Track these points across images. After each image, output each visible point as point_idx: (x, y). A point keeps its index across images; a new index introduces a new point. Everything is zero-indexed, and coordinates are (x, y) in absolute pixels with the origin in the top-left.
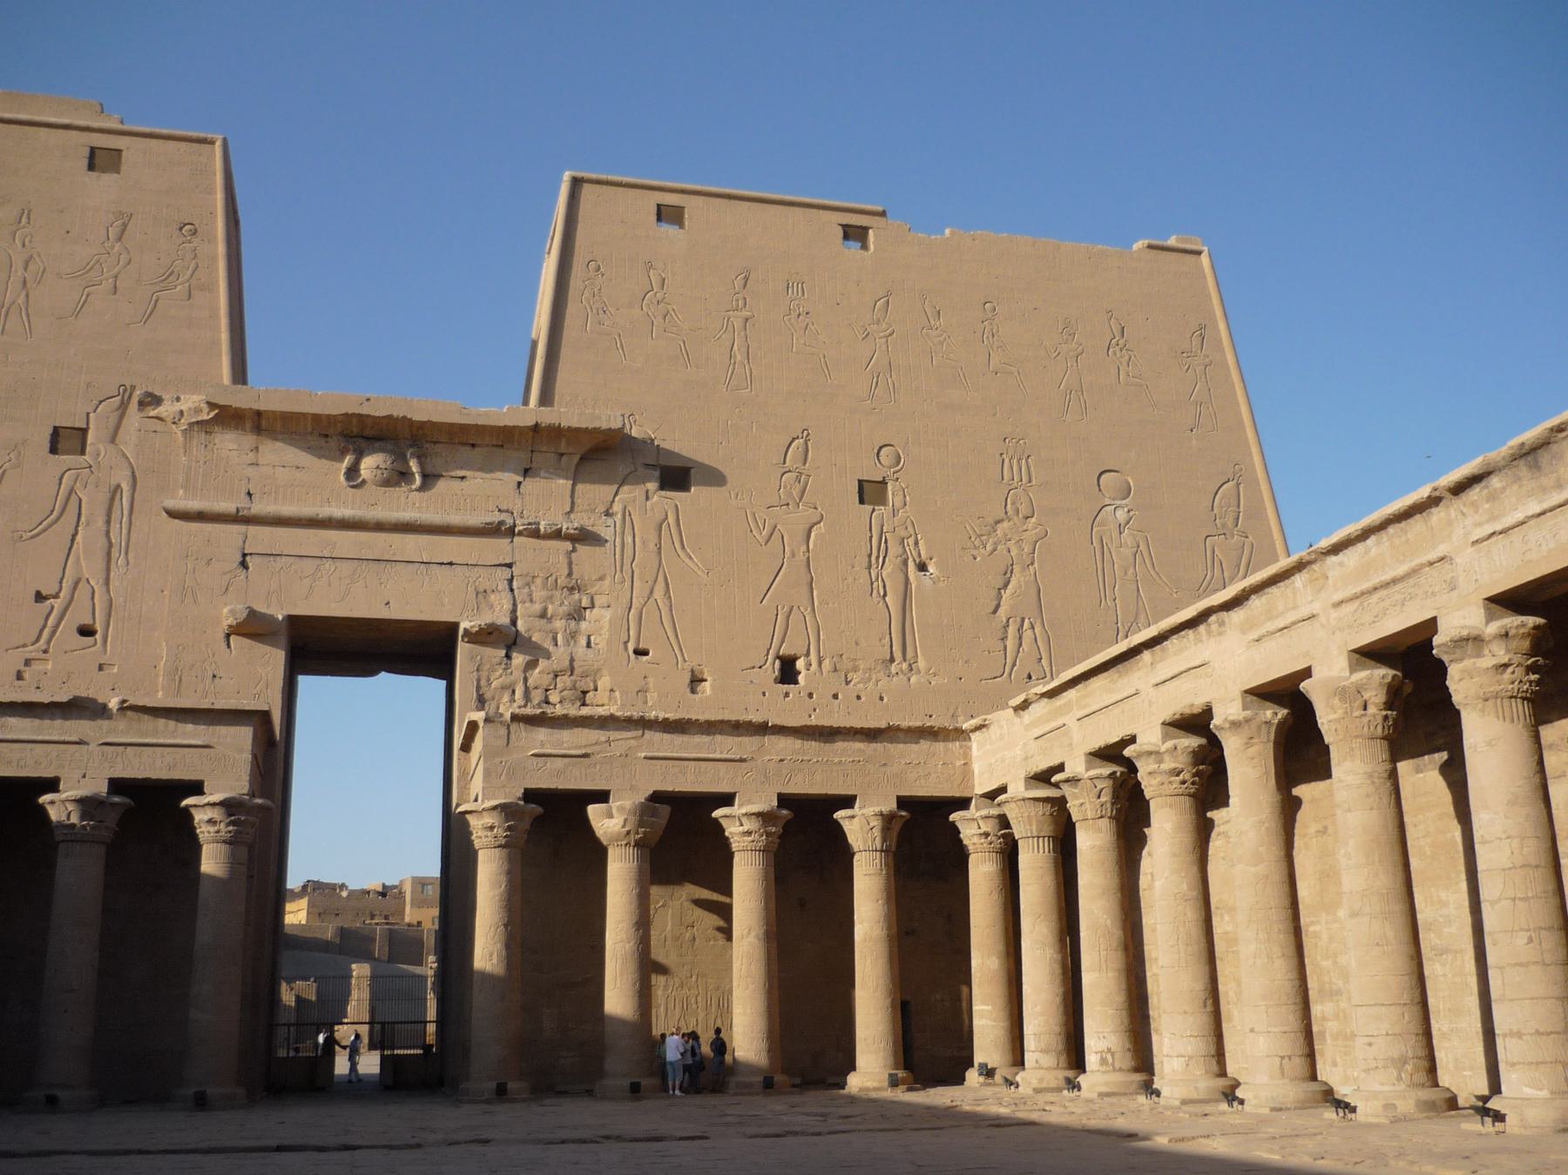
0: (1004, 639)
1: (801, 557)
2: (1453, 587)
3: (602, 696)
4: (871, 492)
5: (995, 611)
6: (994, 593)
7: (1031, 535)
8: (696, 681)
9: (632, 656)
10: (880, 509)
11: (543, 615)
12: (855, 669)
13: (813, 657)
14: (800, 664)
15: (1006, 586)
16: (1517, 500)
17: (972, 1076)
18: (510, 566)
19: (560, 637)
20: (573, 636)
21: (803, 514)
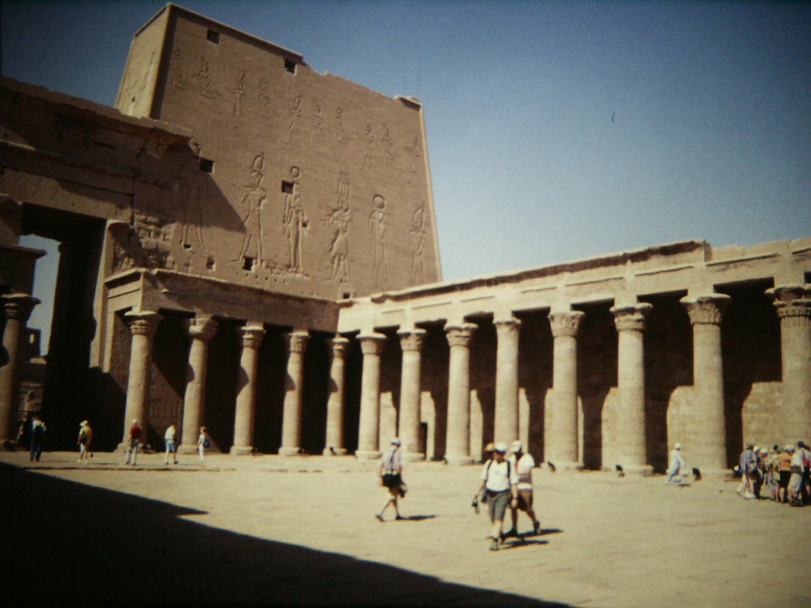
0: (333, 263)
1: (257, 213)
2: (624, 288)
3: (169, 265)
4: (287, 187)
5: (331, 250)
6: (331, 242)
7: (347, 218)
8: (210, 263)
9: (183, 248)
10: (289, 195)
11: (145, 222)
12: (275, 267)
13: (259, 261)
14: (254, 262)
15: (334, 240)
16: (655, 264)
17: (327, 451)
18: (132, 195)
19: (152, 234)
20: (158, 234)
21: (258, 193)
